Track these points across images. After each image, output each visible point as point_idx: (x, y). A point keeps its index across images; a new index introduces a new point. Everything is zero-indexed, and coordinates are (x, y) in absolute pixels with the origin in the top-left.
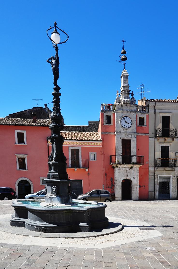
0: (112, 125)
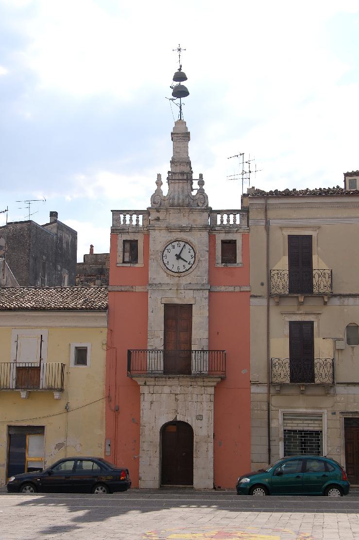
0: (140, 264)
